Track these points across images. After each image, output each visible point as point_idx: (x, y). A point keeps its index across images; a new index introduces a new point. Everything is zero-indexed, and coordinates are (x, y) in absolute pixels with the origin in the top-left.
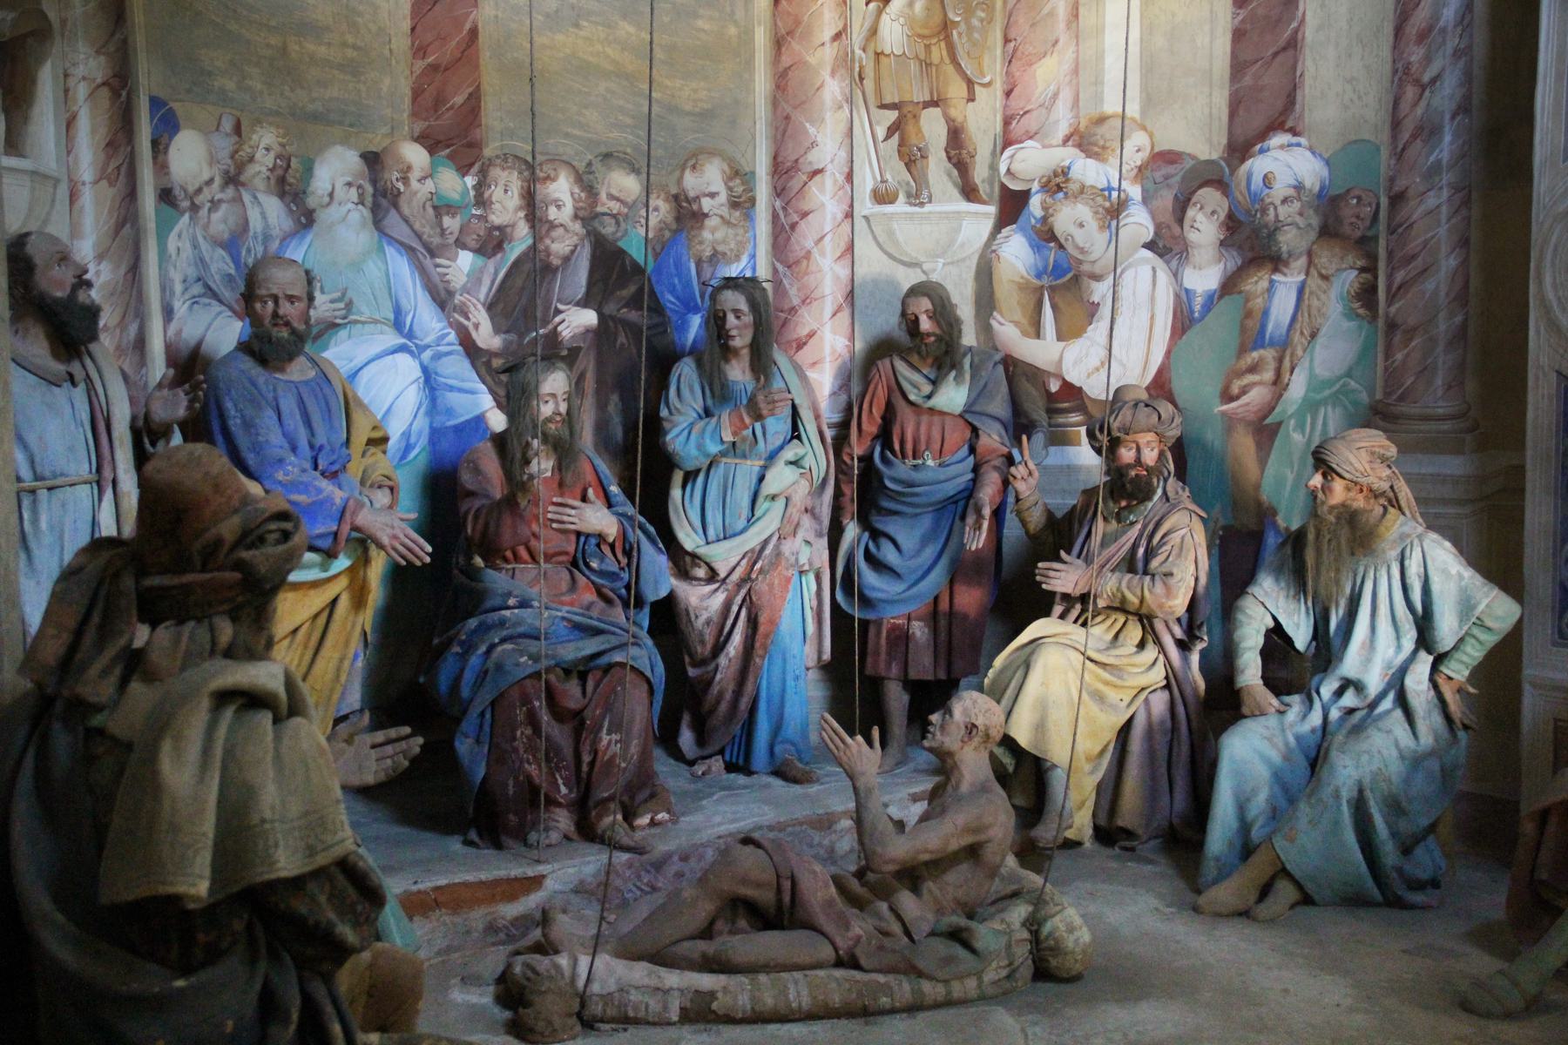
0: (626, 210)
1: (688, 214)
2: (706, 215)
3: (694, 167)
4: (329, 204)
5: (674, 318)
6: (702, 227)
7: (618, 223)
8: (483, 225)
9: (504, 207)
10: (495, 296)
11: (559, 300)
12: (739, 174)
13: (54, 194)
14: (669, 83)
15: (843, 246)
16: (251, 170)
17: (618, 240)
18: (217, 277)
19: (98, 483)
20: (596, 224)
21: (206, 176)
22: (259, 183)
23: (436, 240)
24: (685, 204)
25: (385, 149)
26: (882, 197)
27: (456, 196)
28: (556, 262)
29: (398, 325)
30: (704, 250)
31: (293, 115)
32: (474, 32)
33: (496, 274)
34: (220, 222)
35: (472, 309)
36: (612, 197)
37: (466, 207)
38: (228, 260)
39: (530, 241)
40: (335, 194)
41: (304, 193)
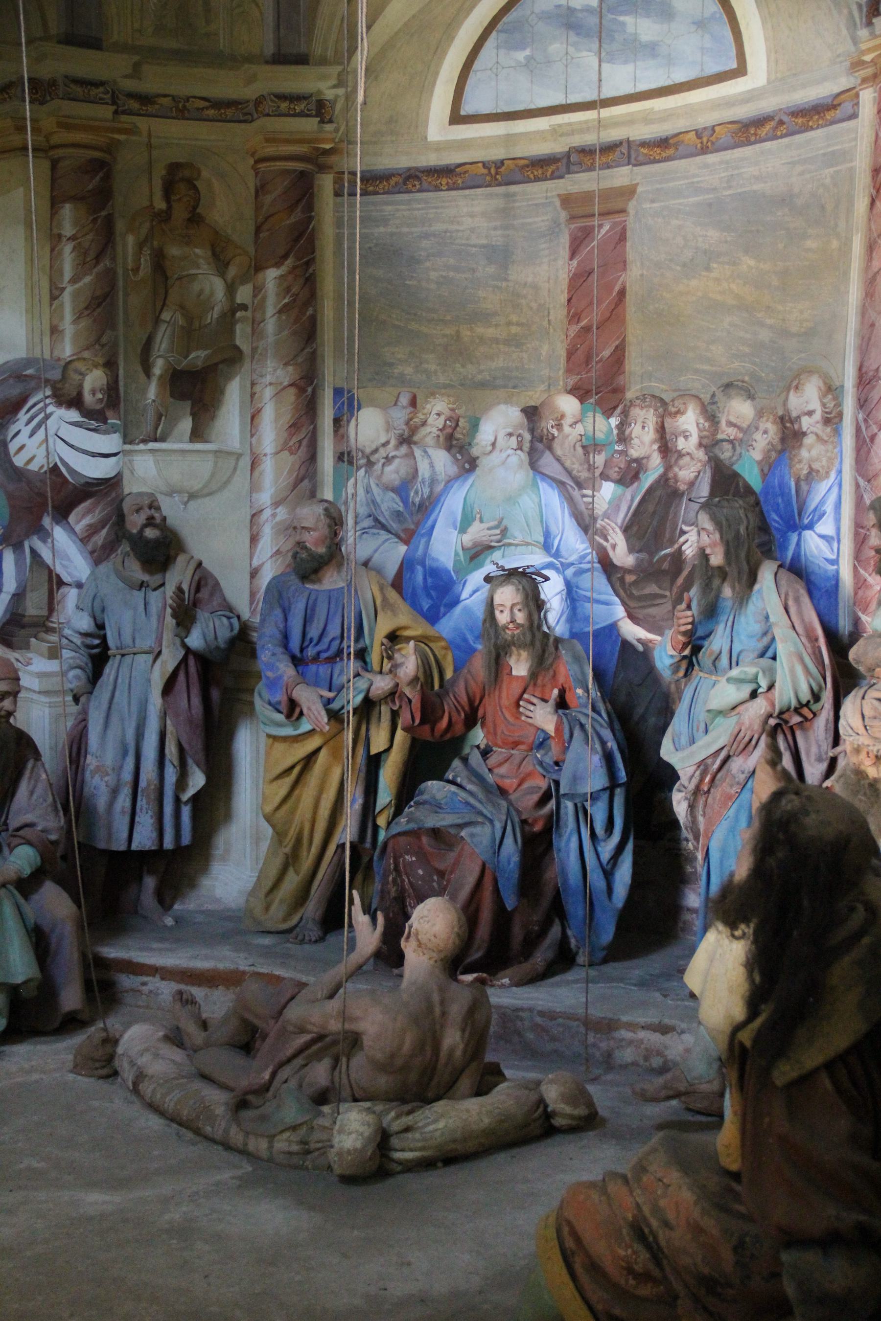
0: (740, 435)
2: (804, 434)
3: (797, 388)
4: (491, 452)
5: (777, 535)
6: (801, 445)
7: (734, 448)
8: (623, 458)
9: (642, 443)
10: (631, 519)
11: (684, 522)
12: (832, 390)
13: (237, 464)
14: (780, 308)
16: (423, 431)
18: (386, 514)
19: (135, 654)
20: (717, 451)
21: (383, 440)
22: (429, 440)
23: (584, 475)
24: (788, 425)
25: (543, 403)
28: (682, 487)
29: (547, 546)
30: (802, 469)
31: (462, 385)
32: (622, 293)
33: (632, 500)
34: (393, 473)
35: (611, 531)
36: (730, 424)
37: (610, 444)
38: (398, 500)
39: (661, 470)
40: (498, 445)
41: (470, 444)
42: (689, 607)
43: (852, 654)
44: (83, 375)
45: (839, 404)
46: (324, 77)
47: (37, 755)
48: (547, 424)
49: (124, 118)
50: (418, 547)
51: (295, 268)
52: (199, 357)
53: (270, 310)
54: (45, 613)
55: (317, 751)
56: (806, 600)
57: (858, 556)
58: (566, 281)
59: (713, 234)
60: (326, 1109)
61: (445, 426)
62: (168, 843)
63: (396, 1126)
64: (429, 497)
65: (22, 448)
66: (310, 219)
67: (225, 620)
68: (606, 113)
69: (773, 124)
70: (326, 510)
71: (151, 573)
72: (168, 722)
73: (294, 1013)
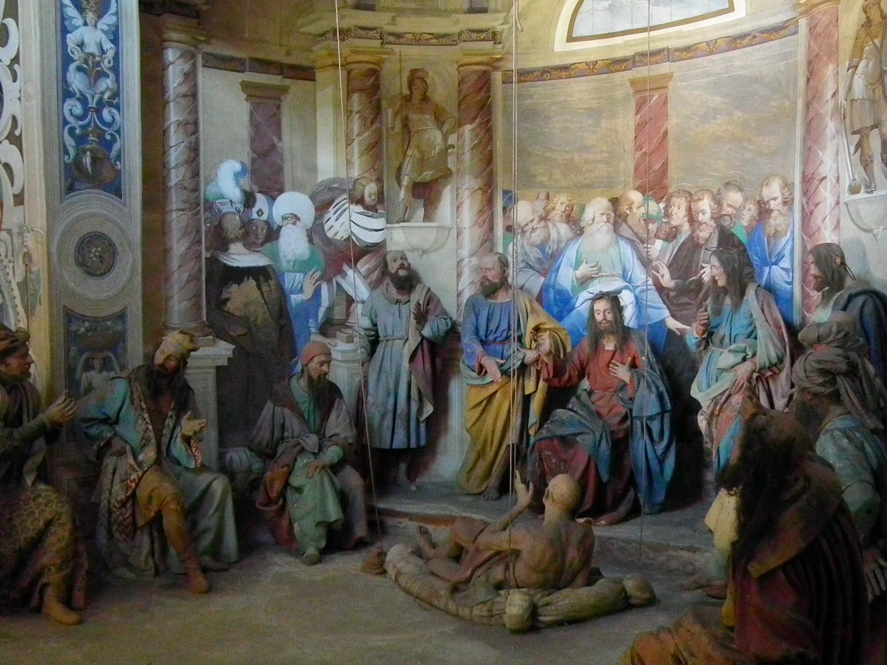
1: (764, 211)
2: (772, 210)
3: (767, 184)
5: (757, 269)
6: (770, 218)
7: (731, 219)
11: (703, 262)
12: (787, 185)
13: (449, 234)
15: (835, 223)
17: (732, 228)
21: (531, 219)
22: (557, 218)
23: (645, 236)
26: (854, 190)
27: (655, 214)
28: (702, 242)
29: (624, 277)
31: (576, 187)
32: (666, 133)
33: (673, 250)
34: (537, 237)
35: (661, 267)
38: (539, 251)
39: (689, 233)
42: (706, 310)
43: (800, 336)
44: (364, 186)
45: (791, 194)
46: (496, 19)
47: (340, 396)
48: (624, 208)
49: (387, 46)
50: (550, 279)
51: (481, 124)
52: (428, 175)
53: (467, 148)
54: (345, 317)
55: (496, 392)
56: (774, 305)
57: (804, 280)
58: (634, 127)
59: (718, 100)
60: (502, 592)
61: (565, 210)
62: (413, 445)
63: (540, 604)
64: (557, 250)
65: (332, 226)
66: (489, 97)
67: (443, 320)
68: (653, 33)
69: (750, 37)
70: (499, 258)
71: (403, 295)
72: (412, 376)
73: (483, 539)
